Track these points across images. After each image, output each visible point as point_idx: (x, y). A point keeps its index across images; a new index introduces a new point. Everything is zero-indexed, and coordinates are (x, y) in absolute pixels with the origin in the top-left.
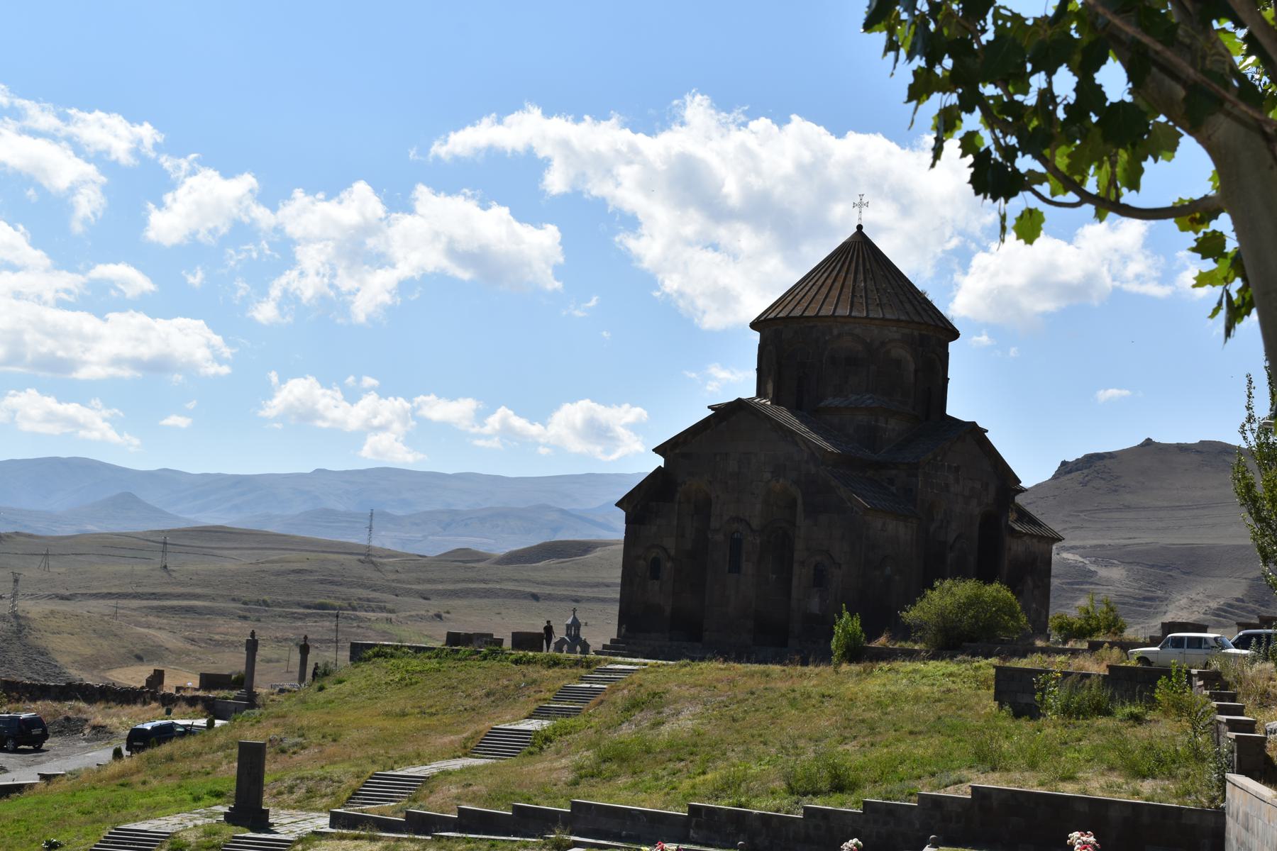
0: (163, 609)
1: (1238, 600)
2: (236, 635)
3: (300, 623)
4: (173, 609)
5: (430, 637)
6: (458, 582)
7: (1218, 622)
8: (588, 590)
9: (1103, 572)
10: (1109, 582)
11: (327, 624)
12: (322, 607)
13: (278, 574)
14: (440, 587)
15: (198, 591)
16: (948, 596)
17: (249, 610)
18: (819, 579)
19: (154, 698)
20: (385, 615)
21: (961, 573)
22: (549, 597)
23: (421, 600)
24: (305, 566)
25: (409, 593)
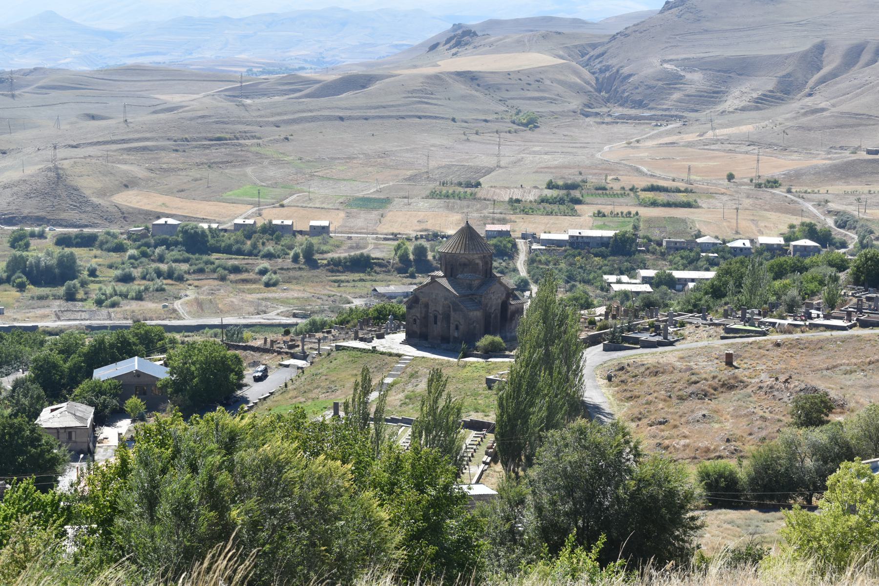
0: (130, 150)
1: (771, 91)
2: (174, 163)
3: (208, 151)
5: (283, 154)
6: (295, 113)
7: (757, 107)
8: (373, 111)
9: (689, 76)
10: (692, 82)
11: (223, 150)
12: (219, 139)
13: (191, 119)
14: (285, 117)
15: (148, 135)
16: (485, 340)
17: (178, 145)
18: (457, 328)
19: (275, 351)
20: (255, 141)
22: (350, 118)
23: (275, 128)
24: (206, 113)
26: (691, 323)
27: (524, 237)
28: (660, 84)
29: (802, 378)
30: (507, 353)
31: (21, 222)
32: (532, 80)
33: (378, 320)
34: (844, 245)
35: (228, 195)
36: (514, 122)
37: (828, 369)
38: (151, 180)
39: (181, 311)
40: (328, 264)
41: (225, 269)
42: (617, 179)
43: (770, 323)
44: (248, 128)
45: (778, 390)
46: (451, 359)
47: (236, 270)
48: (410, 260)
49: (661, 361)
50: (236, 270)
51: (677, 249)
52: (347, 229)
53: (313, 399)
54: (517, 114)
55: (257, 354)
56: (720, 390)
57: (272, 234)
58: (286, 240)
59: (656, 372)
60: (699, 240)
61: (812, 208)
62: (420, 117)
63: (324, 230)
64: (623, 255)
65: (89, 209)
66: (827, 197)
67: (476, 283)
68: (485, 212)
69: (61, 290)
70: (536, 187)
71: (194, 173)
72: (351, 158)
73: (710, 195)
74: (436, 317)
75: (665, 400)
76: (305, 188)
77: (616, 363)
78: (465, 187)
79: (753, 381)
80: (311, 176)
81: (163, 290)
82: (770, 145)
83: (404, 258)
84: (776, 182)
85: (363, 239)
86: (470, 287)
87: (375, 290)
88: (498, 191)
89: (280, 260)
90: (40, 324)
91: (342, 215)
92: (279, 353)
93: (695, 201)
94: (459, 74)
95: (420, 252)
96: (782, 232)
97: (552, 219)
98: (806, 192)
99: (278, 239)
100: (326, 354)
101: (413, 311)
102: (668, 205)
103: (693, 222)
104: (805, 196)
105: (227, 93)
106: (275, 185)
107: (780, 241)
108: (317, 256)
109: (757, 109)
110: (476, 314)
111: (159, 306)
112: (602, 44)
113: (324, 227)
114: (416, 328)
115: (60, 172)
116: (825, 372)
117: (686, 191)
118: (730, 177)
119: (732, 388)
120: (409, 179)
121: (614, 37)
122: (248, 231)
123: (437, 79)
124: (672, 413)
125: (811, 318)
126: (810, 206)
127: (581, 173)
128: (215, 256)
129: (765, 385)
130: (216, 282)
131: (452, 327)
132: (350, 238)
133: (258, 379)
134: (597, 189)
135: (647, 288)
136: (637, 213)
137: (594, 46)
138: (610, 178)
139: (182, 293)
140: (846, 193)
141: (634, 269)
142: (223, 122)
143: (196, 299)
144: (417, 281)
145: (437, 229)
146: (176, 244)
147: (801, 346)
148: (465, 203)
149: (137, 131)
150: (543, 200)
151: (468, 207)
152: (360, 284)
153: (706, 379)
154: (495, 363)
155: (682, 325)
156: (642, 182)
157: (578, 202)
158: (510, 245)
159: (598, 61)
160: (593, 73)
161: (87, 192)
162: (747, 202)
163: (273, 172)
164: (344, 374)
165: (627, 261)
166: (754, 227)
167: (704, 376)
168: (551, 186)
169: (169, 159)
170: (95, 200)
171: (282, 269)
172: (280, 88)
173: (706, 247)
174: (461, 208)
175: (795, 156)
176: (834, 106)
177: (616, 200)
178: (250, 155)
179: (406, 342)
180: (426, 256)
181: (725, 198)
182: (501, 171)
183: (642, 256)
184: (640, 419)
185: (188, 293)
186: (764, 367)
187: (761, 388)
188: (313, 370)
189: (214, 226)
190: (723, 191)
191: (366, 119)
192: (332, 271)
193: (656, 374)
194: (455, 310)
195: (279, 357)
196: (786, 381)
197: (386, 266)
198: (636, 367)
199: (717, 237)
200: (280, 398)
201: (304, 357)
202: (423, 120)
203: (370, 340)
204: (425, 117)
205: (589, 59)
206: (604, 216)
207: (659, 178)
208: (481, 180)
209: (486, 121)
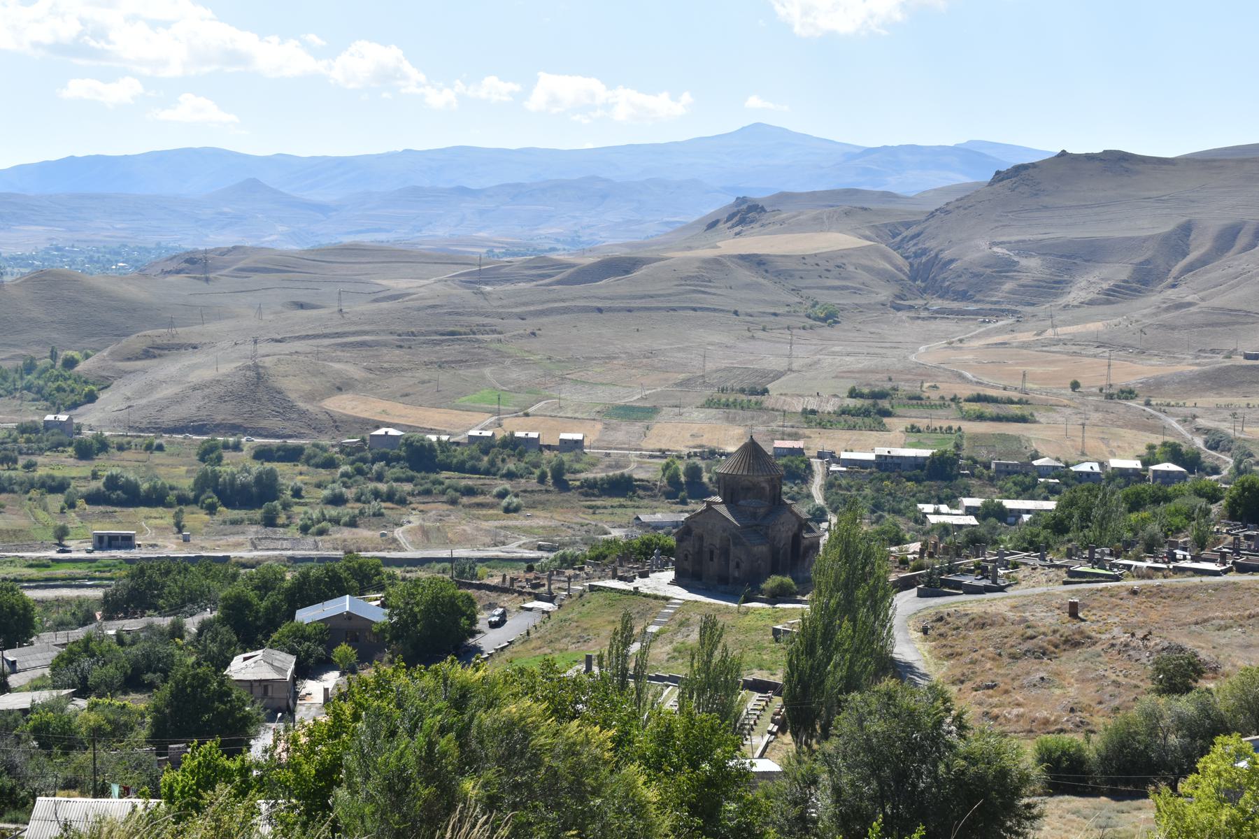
0: (344, 346)
1: (1124, 281)
3: (438, 348)
4: (353, 345)
6: (544, 302)
9: (1024, 262)
10: (1027, 270)
12: (453, 333)
13: (419, 309)
14: (532, 308)
15: (367, 328)
16: (772, 582)
18: (738, 566)
19: (515, 591)
21: (777, 573)
22: (610, 310)
24: (437, 302)
25: (510, 315)
26: (1026, 564)
27: (821, 456)
28: (989, 271)
29: (1165, 634)
30: (799, 597)
31: (212, 430)
32: (833, 265)
33: (642, 556)
34: (1216, 471)
35: (462, 400)
36: (809, 317)
37: (1197, 623)
38: (369, 381)
39: (402, 541)
40: (582, 486)
41: (456, 490)
42: (935, 387)
43: (1125, 565)
44: (487, 321)
45: (1134, 648)
46: (730, 604)
47: (470, 492)
48: (681, 483)
49: (989, 610)
50: (470, 492)
51: (1009, 473)
52: (604, 444)
53: (561, 651)
54: (814, 306)
55: (494, 595)
56: (1062, 647)
57: (514, 449)
58: (531, 456)
59: (982, 623)
60: (1036, 463)
61: (1176, 425)
62: (694, 309)
63: (577, 444)
64: (943, 479)
65: (295, 416)
66: (1195, 411)
67: (762, 511)
68: (774, 426)
69: (258, 514)
70: (835, 396)
71: (422, 374)
72: (611, 358)
73: (1050, 407)
74: (712, 552)
75: (993, 659)
76: (555, 394)
77: (933, 612)
78: (747, 395)
79: (1103, 637)
80: (563, 379)
81: (382, 515)
82: (1124, 347)
83: (673, 480)
84: (1131, 392)
85: (624, 456)
86: (754, 516)
87: (638, 518)
88: (789, 399)
89: (523, 481)
90: (232, 554)
91: (599, 426)
92: (521, 593)
93: (1032, 415)
94: (743, 258)
95: (694, 472)
96: (1139, 453)
97: (855, 434)
98: (1168, 405)
99: (521, 456)
100: (577, 594)
101: (684, 544)
102: (998, 419)
103: (1028, 440)
104: (1167, 409)
105: (463, 279)
106: (519, 390)
107: (1137, 464)
108: (567, 477)
109: (1108, 302)
110: (762, 549)
111: (377, 534)
112: (917, 223)
113: (577, 442)
114: (687, 565)
115: (261, 370)
116: (1193, 627)
117: (1020, 402)
118: (1075, 386)
119: (1077, 644)
120: (682, 384)
121: (932, 215)
122: (485, 445)
123: (717, 262)
124: (1002, 675)
125: (1176, 560)
126: (1173, 422)
127: (890, 379)
128: (445, 474)
129: (1118, 642)
130: (446, 507)
131: (732, 564)
132: (608, 455)
133: (494, 625)
134: (911, 398)
135: (972, 520)
136: (960, 429)
137: (908, 225)
138: (926, 385)
139: (405, 519)
140: (1218, 407)
141: (956, 497)
142: (457, 314)
143: (421, 527)
144: (688, 508)
145: (714, 445)
146: (398, 459)
147: (1164, 595)
148: (748, 413)
149: (355, 323)
150: (844, 412)
151: (753, 418)
152: (619, 511)
153: (1044, 634)
154: (784, 610)
155: (1016, 566)
156: (965, 391)
157: (888, 414)
158: (803, 466)
159: (912, 243)
160: (907, 258)
161: (292, 396)
162: (1095, 417)
163: (515, 374)
164: (599, 621)
165: (946, 487)
166: (1104, 448)
167: (1042, 629)
168: (853, 394)
169: (392, 356)
170: (302, 405)
171: (525, 491)
172: (527, 272)
173: (1045, 471)
174: (744, 419)
175: (1155, 361)
176: (1203, 299)
177: (931, 411)
178: (488, 353)
179: (676, 582)
180: (700, 478)
181: (1068, 411)
182: (793, 375)
183: (965, 480)
184: (962, 682)
185: (411, 518)
186: (1117, 620)
187: (1113, 645)
188: (561, 615)
189: (444, 438)
190: (1066, 402)
191: (630, 311)
192: (586, 495)
193: (983, 626)
194: (735, 544)
195: (521, 598)
196: (1145, 638)
197: (651, 489)
198: (958, 618)
199: (1058, 459)
200: (521, 648)
201: (551, 599)
202: (699, 313)
203: (631, 580)
204: (701, 309)
205: (902, 240)
206: (919, 431)
207: (987, 385)
208: (769, 386)
209: (775, 314)
